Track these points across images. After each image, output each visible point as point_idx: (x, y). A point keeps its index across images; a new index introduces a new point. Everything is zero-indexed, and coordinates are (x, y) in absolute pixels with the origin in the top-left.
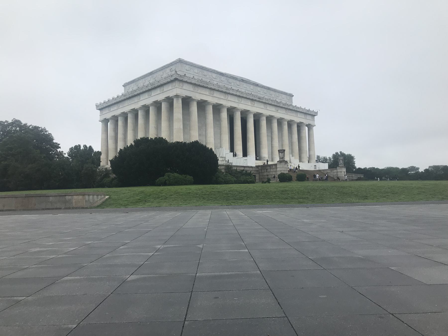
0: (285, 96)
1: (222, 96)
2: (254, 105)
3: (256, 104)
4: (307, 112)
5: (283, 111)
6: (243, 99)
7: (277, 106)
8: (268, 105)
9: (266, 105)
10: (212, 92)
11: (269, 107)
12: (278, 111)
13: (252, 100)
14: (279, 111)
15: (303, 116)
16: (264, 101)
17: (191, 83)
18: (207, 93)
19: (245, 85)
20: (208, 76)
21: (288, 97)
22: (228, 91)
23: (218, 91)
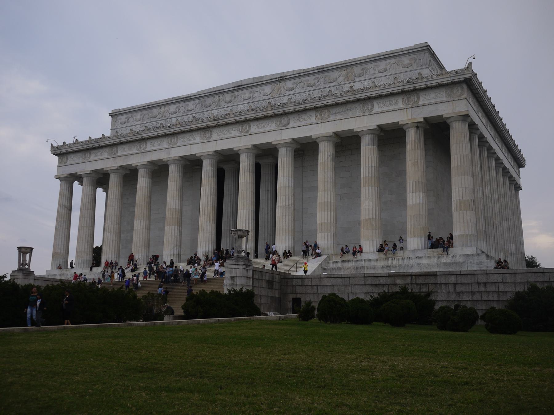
0: (392, 61)
2: (210, 137)
3: (216, 134)
4: (409, 87)
5: (312, 118)
6: (180, 136)
7: (281, 115)
9: (246, 127)
10: (114, 150)
11: (254, 128)
12: (288, 124)
13: (199, 129)
14: (292, 124)
15: (400, 103)
17: (74, 152)
20: (158, 117)
21: (406, 60)
22: (138, 137)
23: (121, 143)
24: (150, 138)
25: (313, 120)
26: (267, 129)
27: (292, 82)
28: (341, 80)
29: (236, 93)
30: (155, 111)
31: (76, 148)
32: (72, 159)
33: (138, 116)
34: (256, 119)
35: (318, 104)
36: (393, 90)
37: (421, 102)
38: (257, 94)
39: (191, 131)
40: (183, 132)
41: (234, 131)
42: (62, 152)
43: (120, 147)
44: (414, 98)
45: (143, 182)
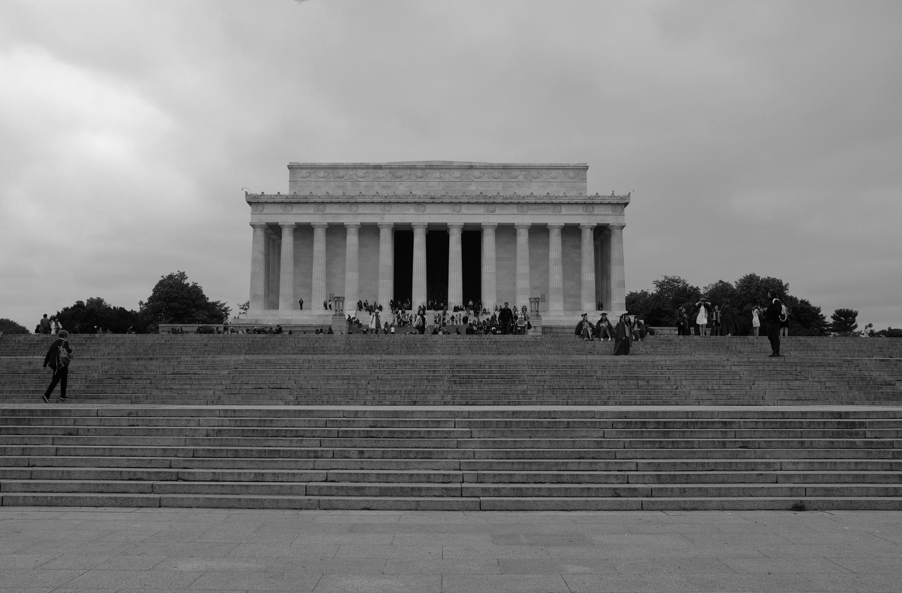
0: (561, 172)
1: (344, 210)
3: (429, 209)
5: (514, 210)
6: (393, 206)
7: (490, 203)
8: (463, 206)
9: (457, 207)
10: (321, 207)
11: (464, 209)
14: (498, 211)
15: (581, 210)
16: (448, 201)
18: (312, 211)
19: (437, 174)
21: (571, 173)
23: (331, 203)
24: (365, 203)
25: (515, 211)
26: (477, 212)
27: (479, 171)
28: (521, 178)
29: (427, 171)
30: (341, 173)
31: (276, 200)
32: (268, 209)
33: (322, 173)
34: (468, 203)
35: (521, 201)
36: (578, 201)
37: (595, 213)
38: (447, 175)
39: (407, 203)
40: (398, 203)
41: (447, 209)
42: (254, 202)
43: (328, 206)
44: (590, 208)
45: (352, 239)
